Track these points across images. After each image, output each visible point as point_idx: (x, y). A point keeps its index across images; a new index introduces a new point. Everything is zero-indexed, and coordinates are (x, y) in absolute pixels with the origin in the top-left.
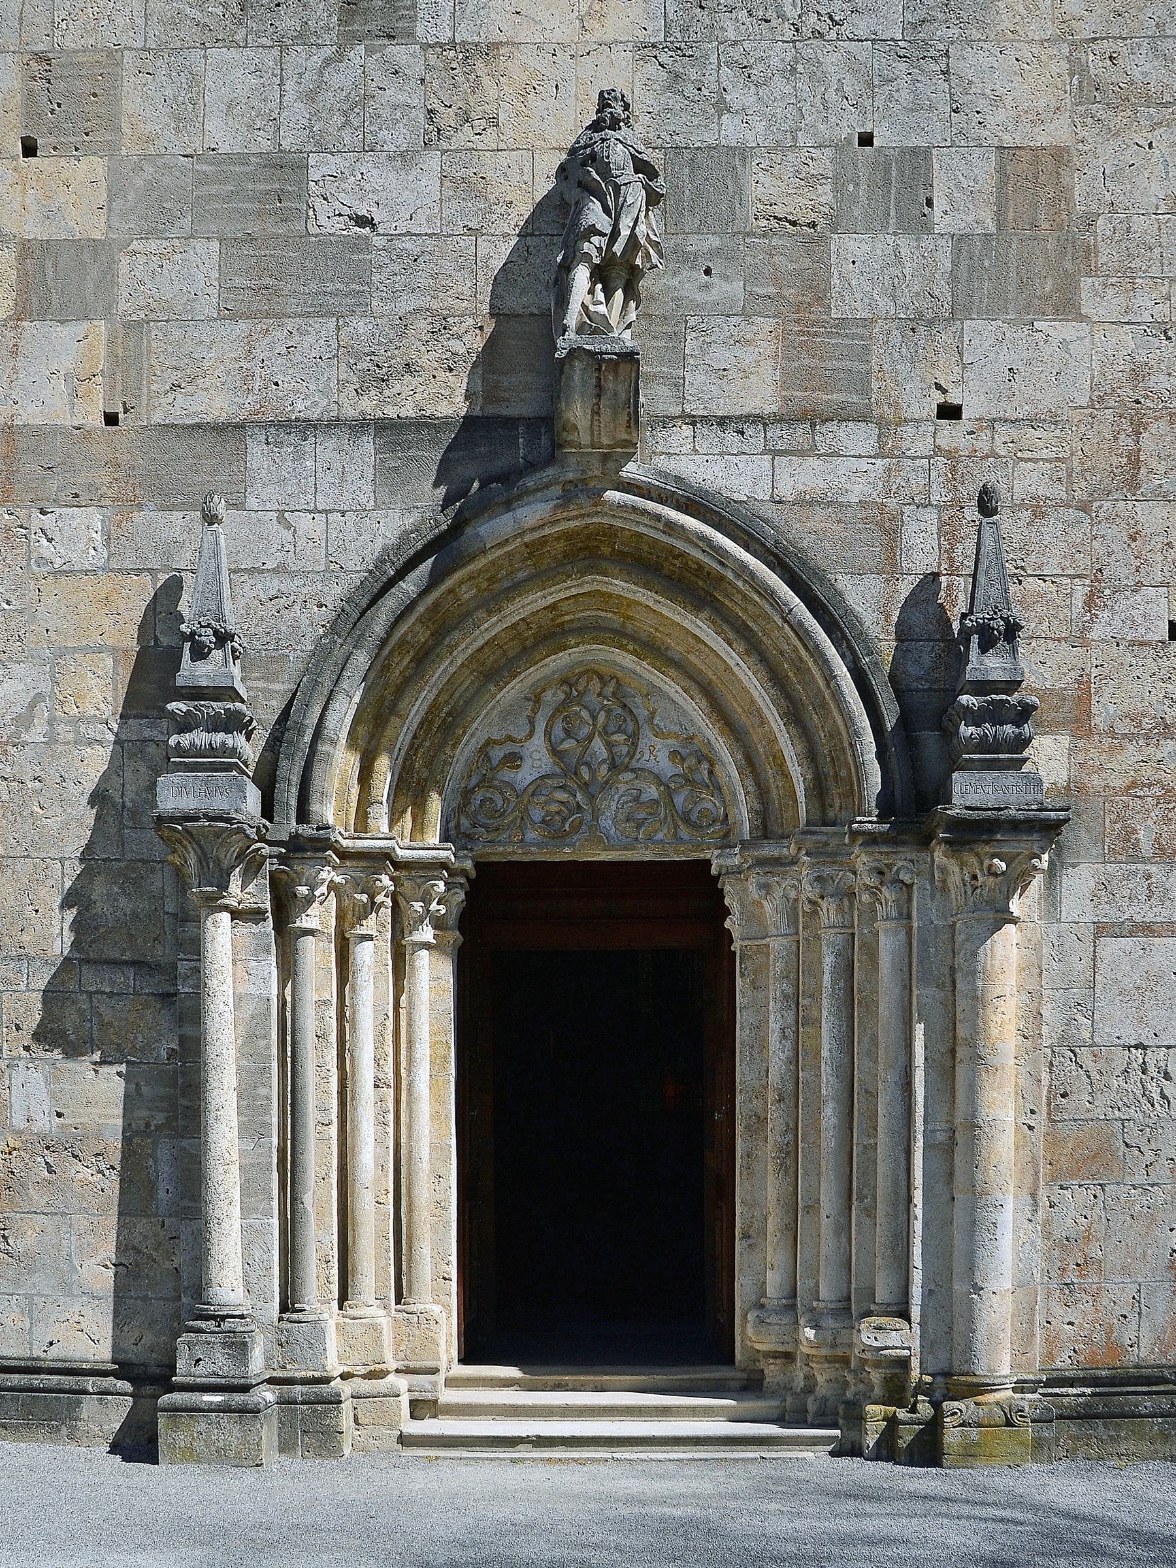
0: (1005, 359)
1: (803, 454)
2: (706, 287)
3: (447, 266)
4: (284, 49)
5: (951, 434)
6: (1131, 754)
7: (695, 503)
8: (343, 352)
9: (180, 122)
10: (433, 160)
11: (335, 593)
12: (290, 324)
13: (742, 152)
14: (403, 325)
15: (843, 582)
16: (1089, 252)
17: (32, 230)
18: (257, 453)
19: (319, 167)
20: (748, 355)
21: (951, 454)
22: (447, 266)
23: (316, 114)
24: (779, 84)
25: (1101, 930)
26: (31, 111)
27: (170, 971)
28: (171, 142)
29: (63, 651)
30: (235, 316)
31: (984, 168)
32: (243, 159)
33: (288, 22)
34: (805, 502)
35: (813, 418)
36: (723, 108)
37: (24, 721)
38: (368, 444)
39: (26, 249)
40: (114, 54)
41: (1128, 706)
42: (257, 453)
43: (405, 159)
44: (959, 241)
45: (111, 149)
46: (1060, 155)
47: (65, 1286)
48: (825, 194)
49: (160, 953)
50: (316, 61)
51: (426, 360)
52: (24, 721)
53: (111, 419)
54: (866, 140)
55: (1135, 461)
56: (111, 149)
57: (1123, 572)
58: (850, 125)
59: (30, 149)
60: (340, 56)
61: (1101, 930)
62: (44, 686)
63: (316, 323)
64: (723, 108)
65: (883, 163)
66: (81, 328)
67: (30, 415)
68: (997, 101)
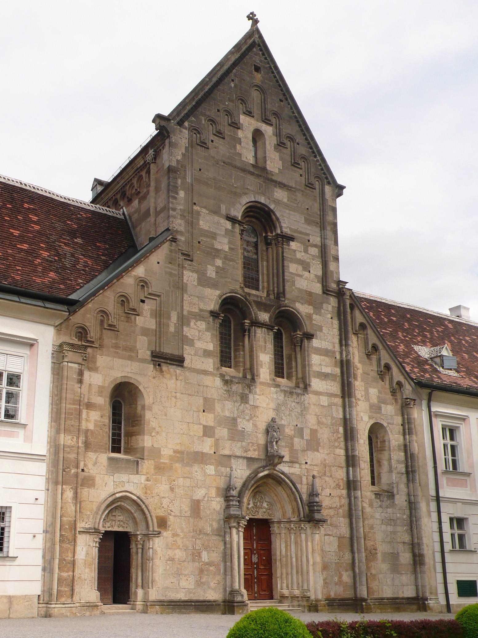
1: (292, 467)
2: (281, 443)
3: (253, 436)
4: (234, 403)
5: (307, 466)
7: (283, 473)
9: (223, 411)
10: (251, 421)
12: (236, 442)
13: (284, 425)
14: (249, 444)
16: (320, 443)
17: (204, 423)
18: (233, 461)
19: (239, 420)
20: (286, 453)
21: (307, 469)
22: (253, 436)
23: (238, 413)
25: (325, 535)
26: (204, 405)
28: (222, 414)
29: (209, 487)
30: (229, 440)
31: (309, 431)
32: (230, 417)
36: (282, 419)
37: (204, 497)
40: (215, 399)
42: (233, 461)
43: (248, 420)
44: (307, 440)
45: (214, 413)
48: (293, 432)
50: (238, 405)
51: (251, 449)
52: (204, 497)
53: (215, 453)
54: (297, 425)
57: (324, 486)
58: (295, 424)
59: (204, 411)
60: (240, 405)
62: (207, 492)
63: (239, 442)
66: (211, 439)
67: (205, 451)
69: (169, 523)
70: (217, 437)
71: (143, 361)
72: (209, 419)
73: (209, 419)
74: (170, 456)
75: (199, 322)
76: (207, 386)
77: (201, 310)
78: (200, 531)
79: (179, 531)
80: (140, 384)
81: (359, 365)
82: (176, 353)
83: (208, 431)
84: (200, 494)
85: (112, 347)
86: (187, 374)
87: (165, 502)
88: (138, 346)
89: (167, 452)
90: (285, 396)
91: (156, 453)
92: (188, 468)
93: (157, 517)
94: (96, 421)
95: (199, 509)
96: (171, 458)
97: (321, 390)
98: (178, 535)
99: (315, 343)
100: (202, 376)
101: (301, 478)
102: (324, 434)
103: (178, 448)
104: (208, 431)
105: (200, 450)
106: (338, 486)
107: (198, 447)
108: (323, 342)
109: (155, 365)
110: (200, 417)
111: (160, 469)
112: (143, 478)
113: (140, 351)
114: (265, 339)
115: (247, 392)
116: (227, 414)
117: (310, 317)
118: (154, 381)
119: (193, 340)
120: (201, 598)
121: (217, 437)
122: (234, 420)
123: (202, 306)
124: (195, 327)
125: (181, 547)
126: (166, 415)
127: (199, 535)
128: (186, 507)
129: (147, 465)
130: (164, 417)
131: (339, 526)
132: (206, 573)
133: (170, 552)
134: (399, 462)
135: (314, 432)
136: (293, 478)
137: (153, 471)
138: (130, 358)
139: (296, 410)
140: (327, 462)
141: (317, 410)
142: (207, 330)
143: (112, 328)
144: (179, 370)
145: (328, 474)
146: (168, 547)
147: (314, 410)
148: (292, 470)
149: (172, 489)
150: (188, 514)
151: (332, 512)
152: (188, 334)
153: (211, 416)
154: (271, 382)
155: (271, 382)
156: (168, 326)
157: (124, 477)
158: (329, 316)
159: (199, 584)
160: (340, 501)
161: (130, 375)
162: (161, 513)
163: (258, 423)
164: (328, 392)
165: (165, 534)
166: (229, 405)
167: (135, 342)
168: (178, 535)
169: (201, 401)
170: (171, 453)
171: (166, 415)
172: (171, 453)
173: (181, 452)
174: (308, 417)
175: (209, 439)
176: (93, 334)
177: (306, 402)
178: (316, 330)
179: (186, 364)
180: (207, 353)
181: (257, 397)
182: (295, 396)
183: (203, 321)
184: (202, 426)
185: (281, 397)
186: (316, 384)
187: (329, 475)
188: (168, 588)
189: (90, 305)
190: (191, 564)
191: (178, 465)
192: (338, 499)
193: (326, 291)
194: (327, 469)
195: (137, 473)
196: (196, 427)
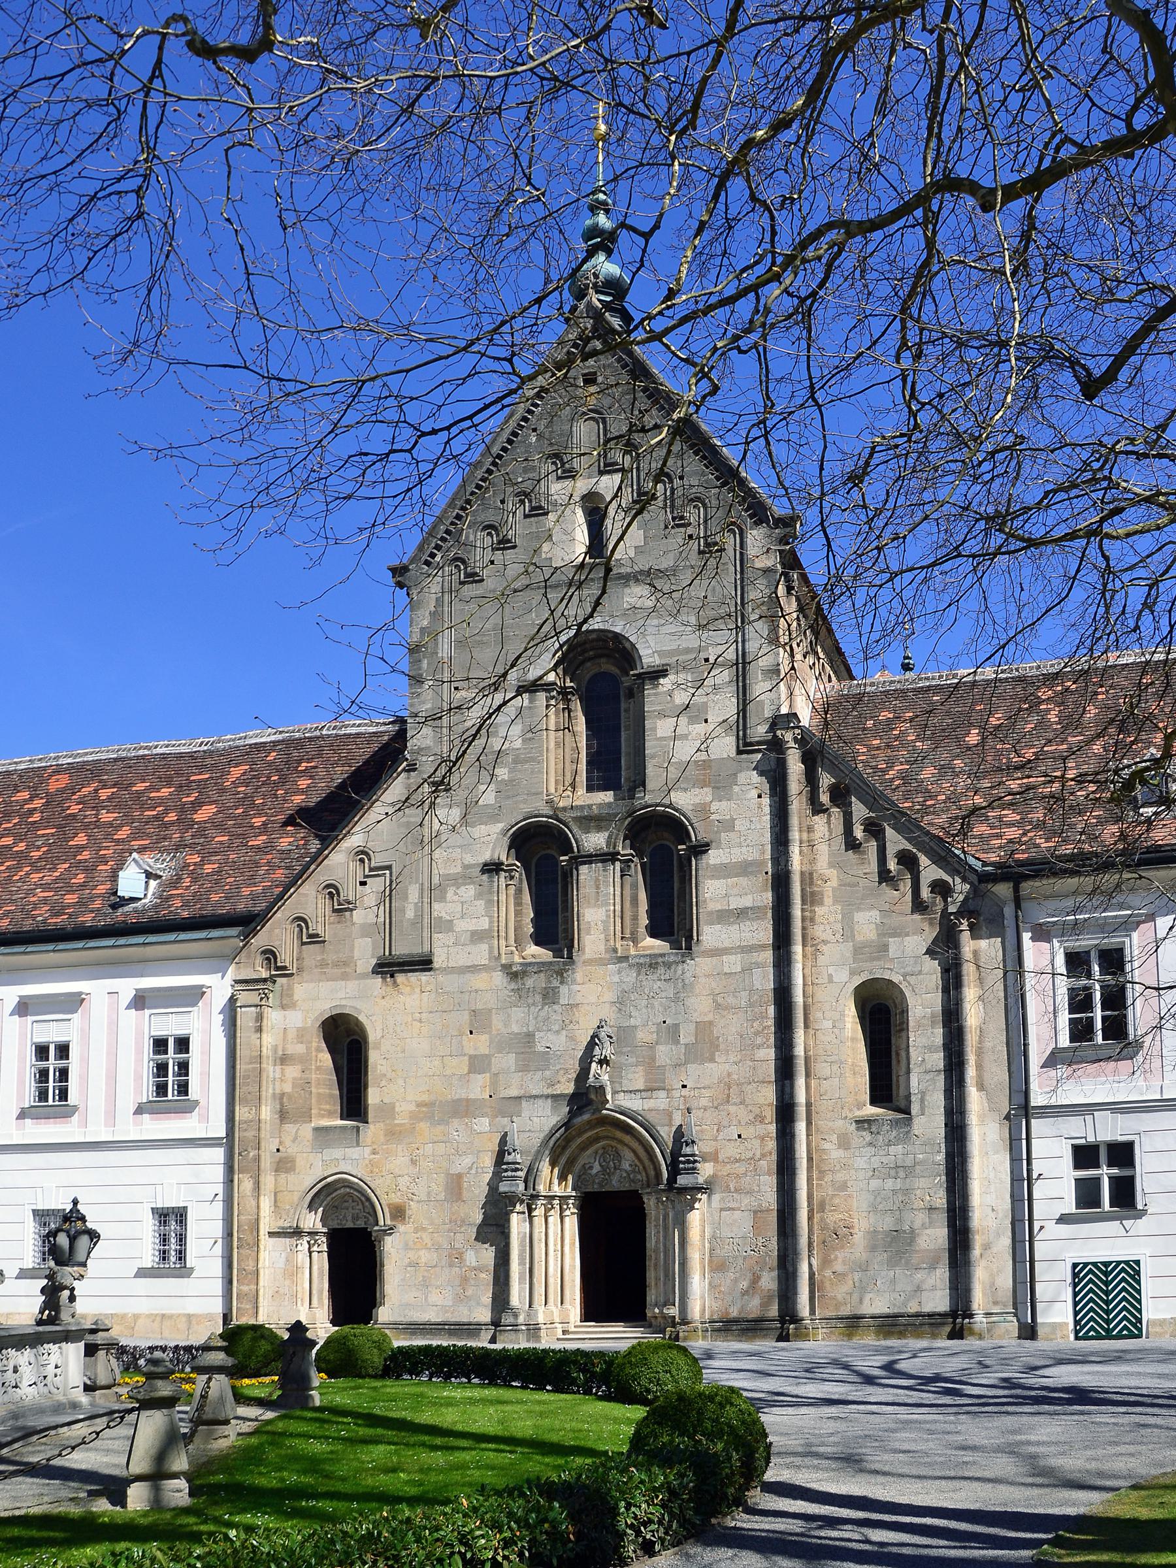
0: (698, 1073)
5: (685, 1092)
6: (728, 1166)
8: (544, 1079)
9: (506, 1026)
10: (564, 1032)
11: (542, 1136)
13: (635, 1027)
15: (659, 1128)
16: (718, 1046)
17: (472, 1052)
20: (637, 1076)
24: (644, 1010)
25: (722, 1210)
26: (471, 1024)
27: (503, 1226)
28: (504, 1031)
31: (692, 1027)
33: (530, 1001)
34: (650, 1110)
35: (652, 1090)
36: (631, 1016)
37: (470, 1168)
38: (549, 1101)
39: (471, 1057)
40: (490, 1010)
41: (728, 1155)
42: (524, 1104)
43: (558, 1032)
44: (686, 1045)
45: (490, 1033)
46: (711, 1023)
47: (478, 1304)
49: (501, 1222)
51: (563, 1080)
52: (470, 1168)
55: (729, 1096)
56: (490, 1033)
57: (725, 1123)
59: (471, 1033)
61: (722, 1210)
64: (631, 1016)
65: (668, 1027)
67: (472, 1096)
68: (696, 1011)
69: (408, 1212)
70: (494, 1070)
71: (363, 976)
72: (481, 1044)
73: (481, 1044)
74: (411, 1112)
75: (463, 888)
76: (476, 991)
77: (466, 867)
78: (463, 1221)
79: (425, 1223)
80: (360, 1012)
81: (832, 874)
82: (416, 950)
83: (477, 1064)
84: (462, 1164)
85: (316, 966)
86: (441, 978)
87: (403, 1182)
88: (357, 954)
89: (404, 1109)
90: (639, 974)
91: (388, 1110)
92: (442, 1127)
93: (389, 1205)
94: (294, 1079)
95: (460, 1188)
96: (414, 1117)
97: (727, 944)
98: (424, 1229)
99: (714, 857)
100: (468, 976)
101: (670, 1115)
102: (730, 1027)
103: (425, 1098)
104: (477, 1064)
105: (464, 1096)
106: (760, 1119)
107: (462, 1094)
108: (735, 851)
109: (384, 979)
110: (464, 1043)
111: (393, 1134)
112: (368, 1150)
113: (359, 963)
114: (597, 880)
115: (555, 983)
116: (515, 1028)
117: (703, 810)
118: (383, 1002)
119: (452, 921)
120: (465, 1320)
121: (494, 1070)
122: (529, 1038)
123: (469, 859)
124: (456, 898)
125: (429, 1245)
126: (403, 1051)
127: (461, 1226)
128: (438, 1187)
129: (372, 1131)
130: (401, 1055)
131: (759, 1191)
132: (473, 1282)
133: (411, 1254)
134: (930, 1049)
135: (703, 1028)
136: (652, 1118)
137: (382, 1139)
138: (345, 977)
139: (664, 994)
140: (735, 1077)
141: (714, 985)
142: (478, 896)
143: (315, 939)
144: (424, 977)
145: (735, 1099)
146: (407, 1247)
147: (704, 985)
148: (649, 1104)
149: (414, 1162)
150: (442, 1196)
151: (741, 1168)
152: (443, 914)
153: (484, 1038)
154: (608, 956)
155: (608, 956)
156: (403, 911)
157: (336, 1153)
158: (754, 793)
159: (460, 1299)
160: (762, 1146)
161: (344, 1002)
162: (396, 1199)
163: (577, 1033)
164: (743, 944)
165: (401, 1228)
166: (518, 1013)
167: (352, 950)
168: (424, 1229)
169: (466, 1016)
170: (413, 1107)
171: (403, 1051)
172: (413, 1107)
173: (430, 1105)
174: (691, 1001)
175: (479, 1076)
176: (286, 957)
177: (688, 975)
178: (718, 832)
179: (438, 962)
180: (477, 937)
181: (578, 987)
182: (661, 970)
183: (469, 884)
184: (466, 1058)
185: (630, 977)
186: (710, 935)
187: (738, 1100)
188: (408, 1305)
189: (278, 915)
190: (447, 1270)
191: (423, 1125)
192: (757, 1143)
193: (744, 747)
194: (734, 1090)
195: (358, 1145)
196: (455, 1061)
